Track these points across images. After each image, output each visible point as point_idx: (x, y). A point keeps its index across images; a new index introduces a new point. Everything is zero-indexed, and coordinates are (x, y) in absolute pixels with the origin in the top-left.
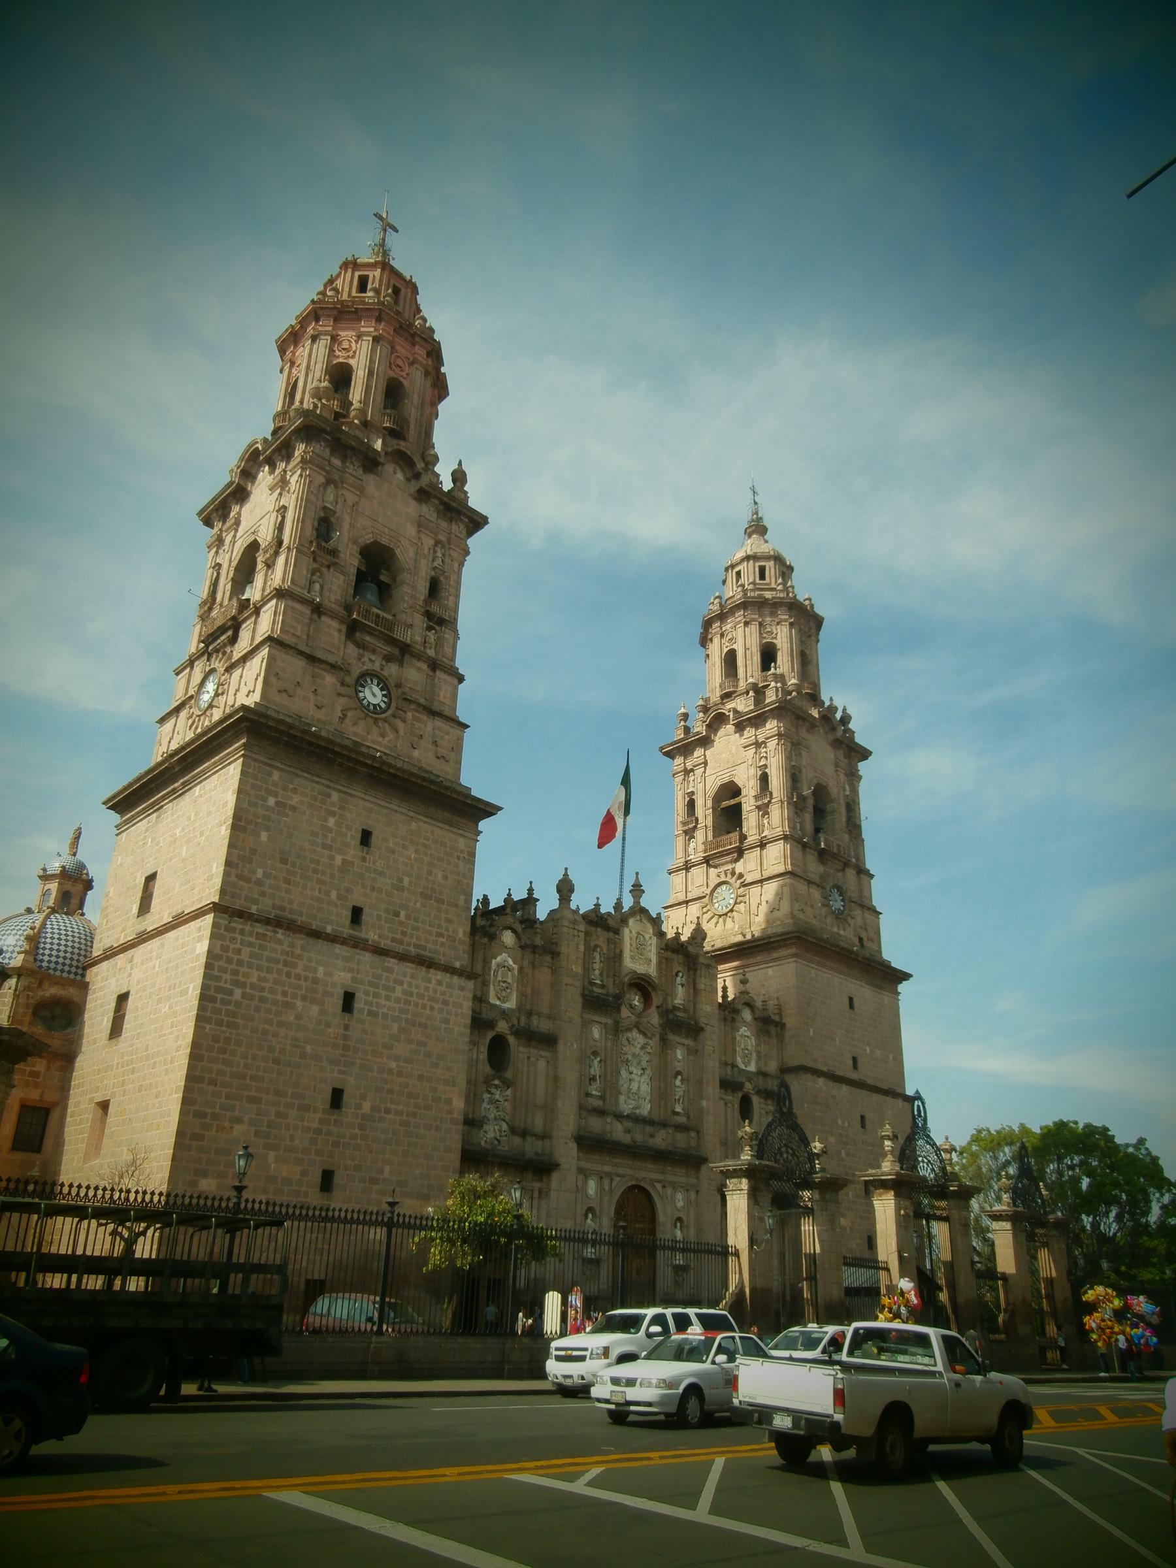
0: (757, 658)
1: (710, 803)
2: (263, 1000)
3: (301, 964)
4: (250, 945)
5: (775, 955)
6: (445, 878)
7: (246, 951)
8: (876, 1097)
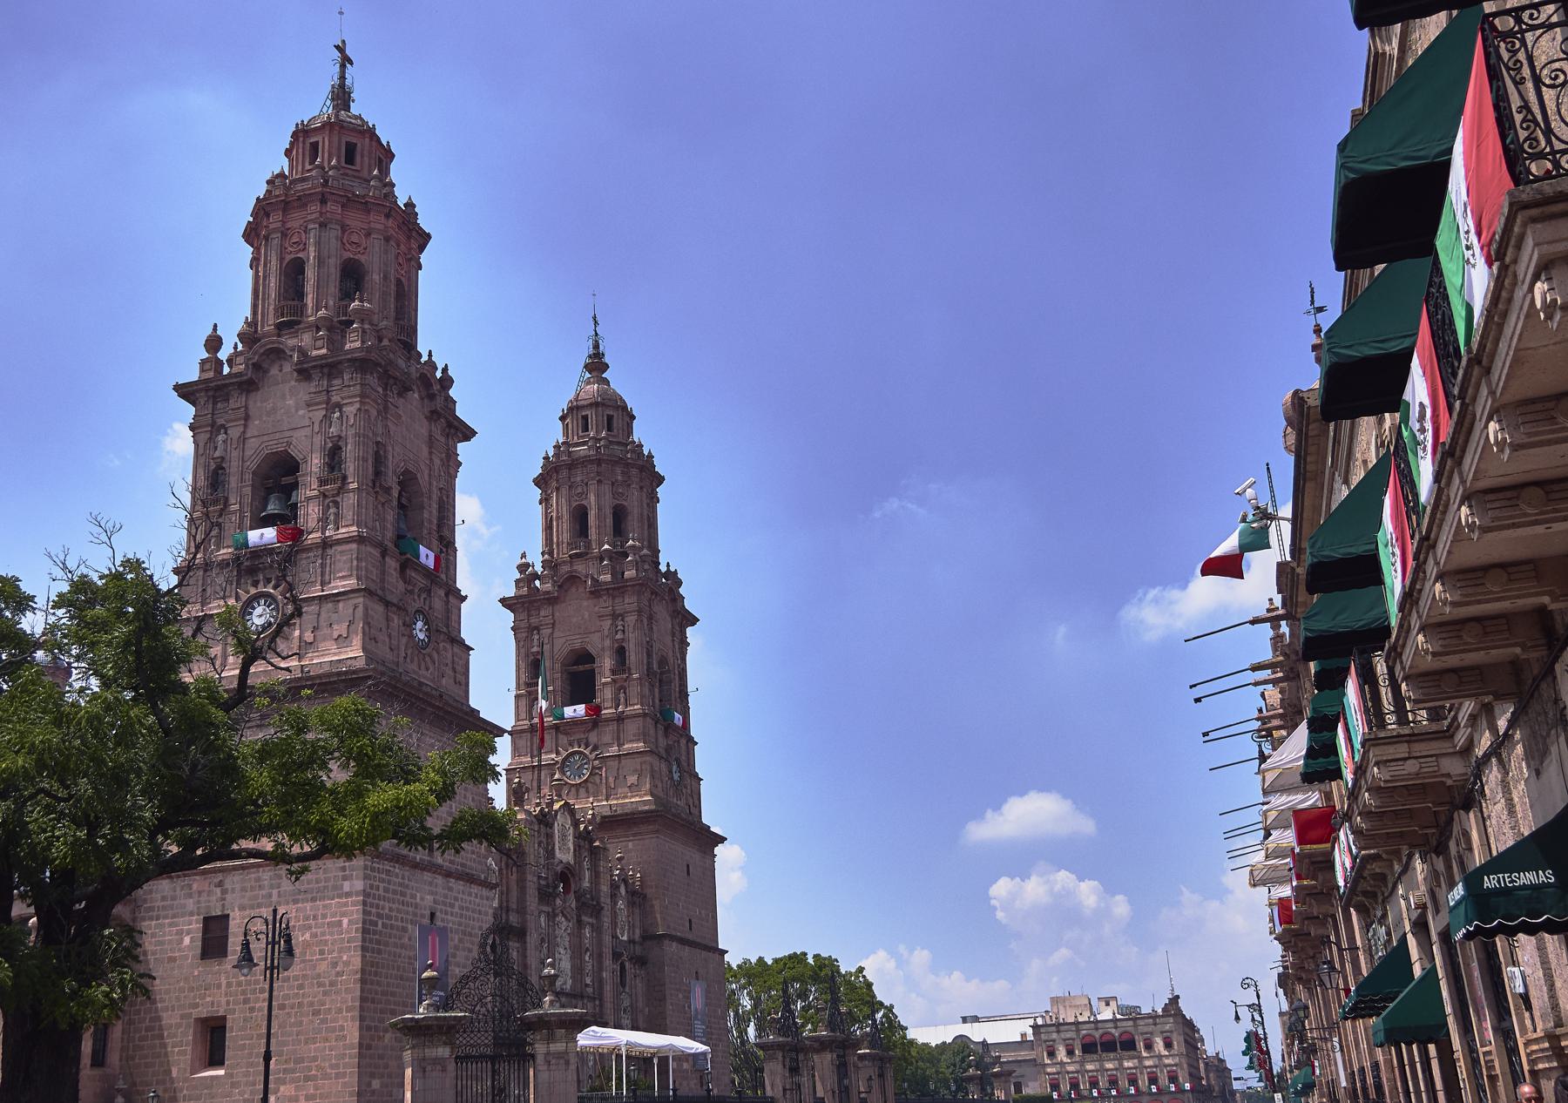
0: (609, 521)
1: (558, 666)
2: (392, 927)
3: (409, 892)
4: (383, 881)
5: (635, 830)
6: (473, 799)
7: (381, 885)
8: (704, 954)
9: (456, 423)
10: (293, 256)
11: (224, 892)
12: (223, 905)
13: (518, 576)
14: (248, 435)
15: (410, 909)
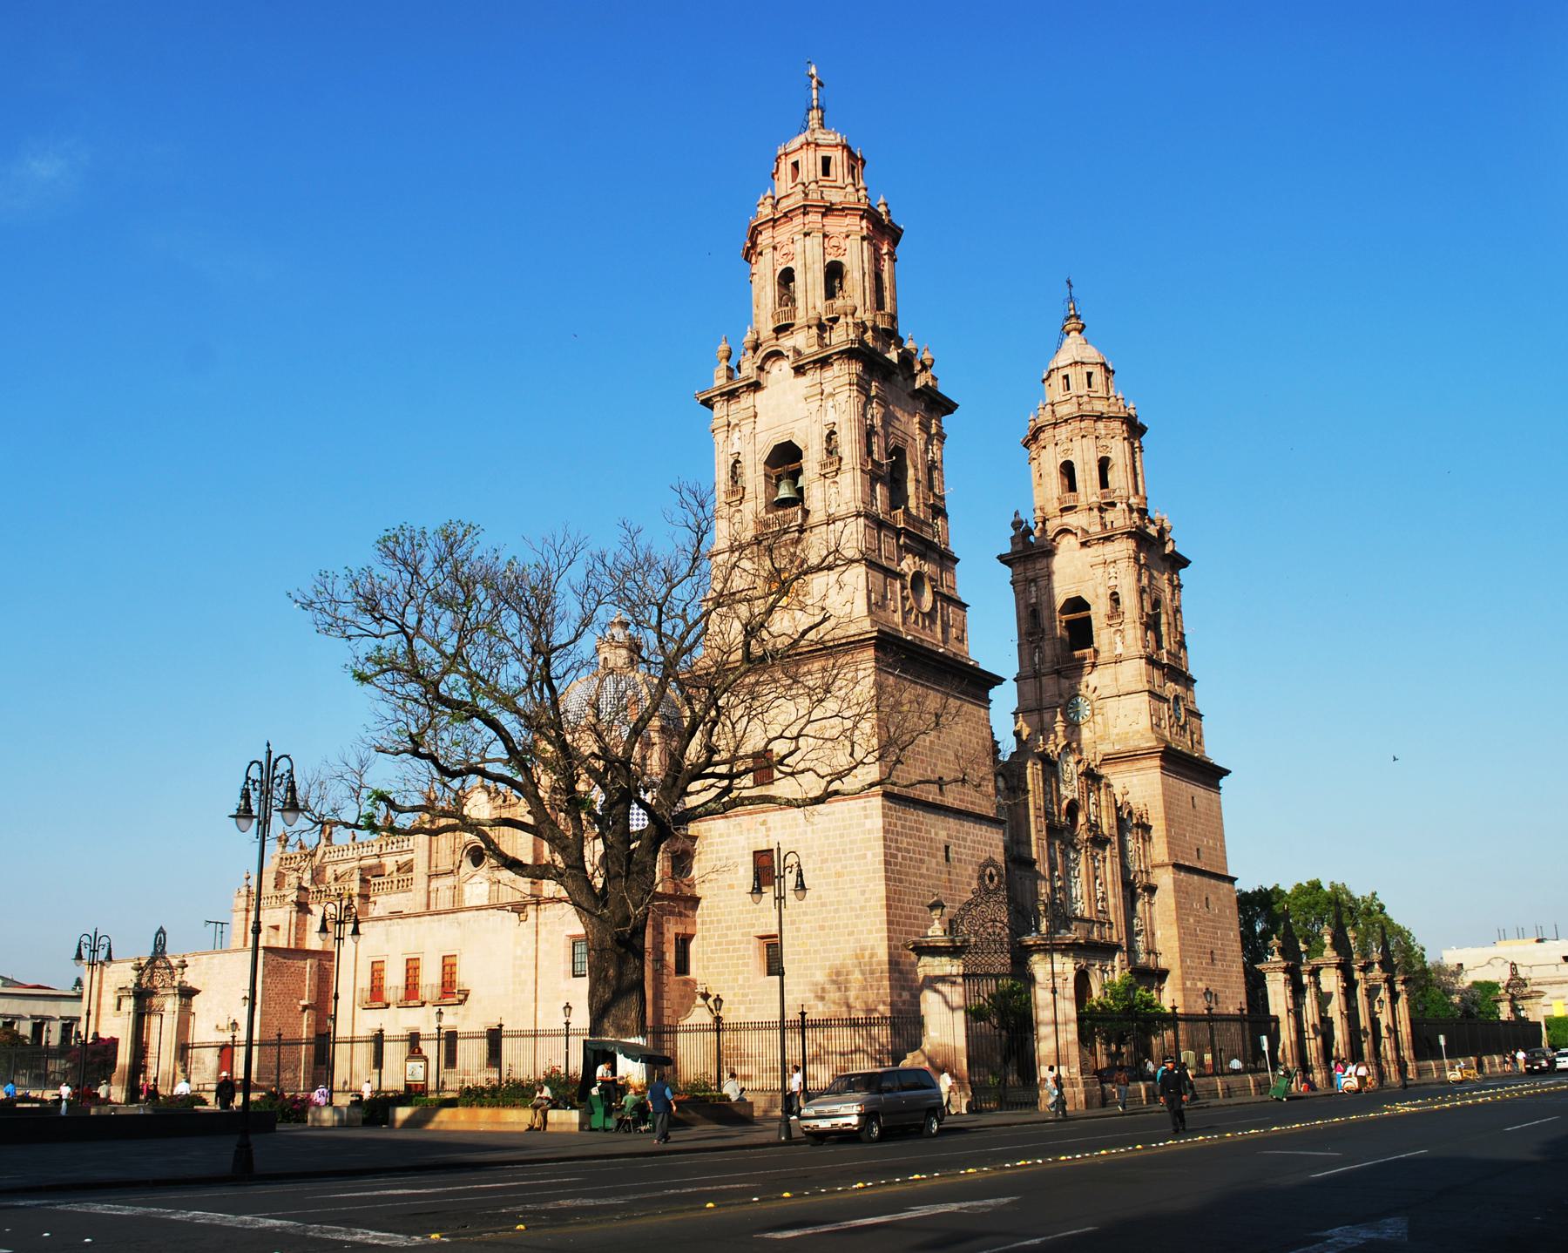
4: (900, 818)
7: (899, 823)
9: (938, 398)
10: (784, 267)
11: (768, 830)
12: (768, 841)
13: (1013, 533)
14: (757, 431)
15: (926, 843)
